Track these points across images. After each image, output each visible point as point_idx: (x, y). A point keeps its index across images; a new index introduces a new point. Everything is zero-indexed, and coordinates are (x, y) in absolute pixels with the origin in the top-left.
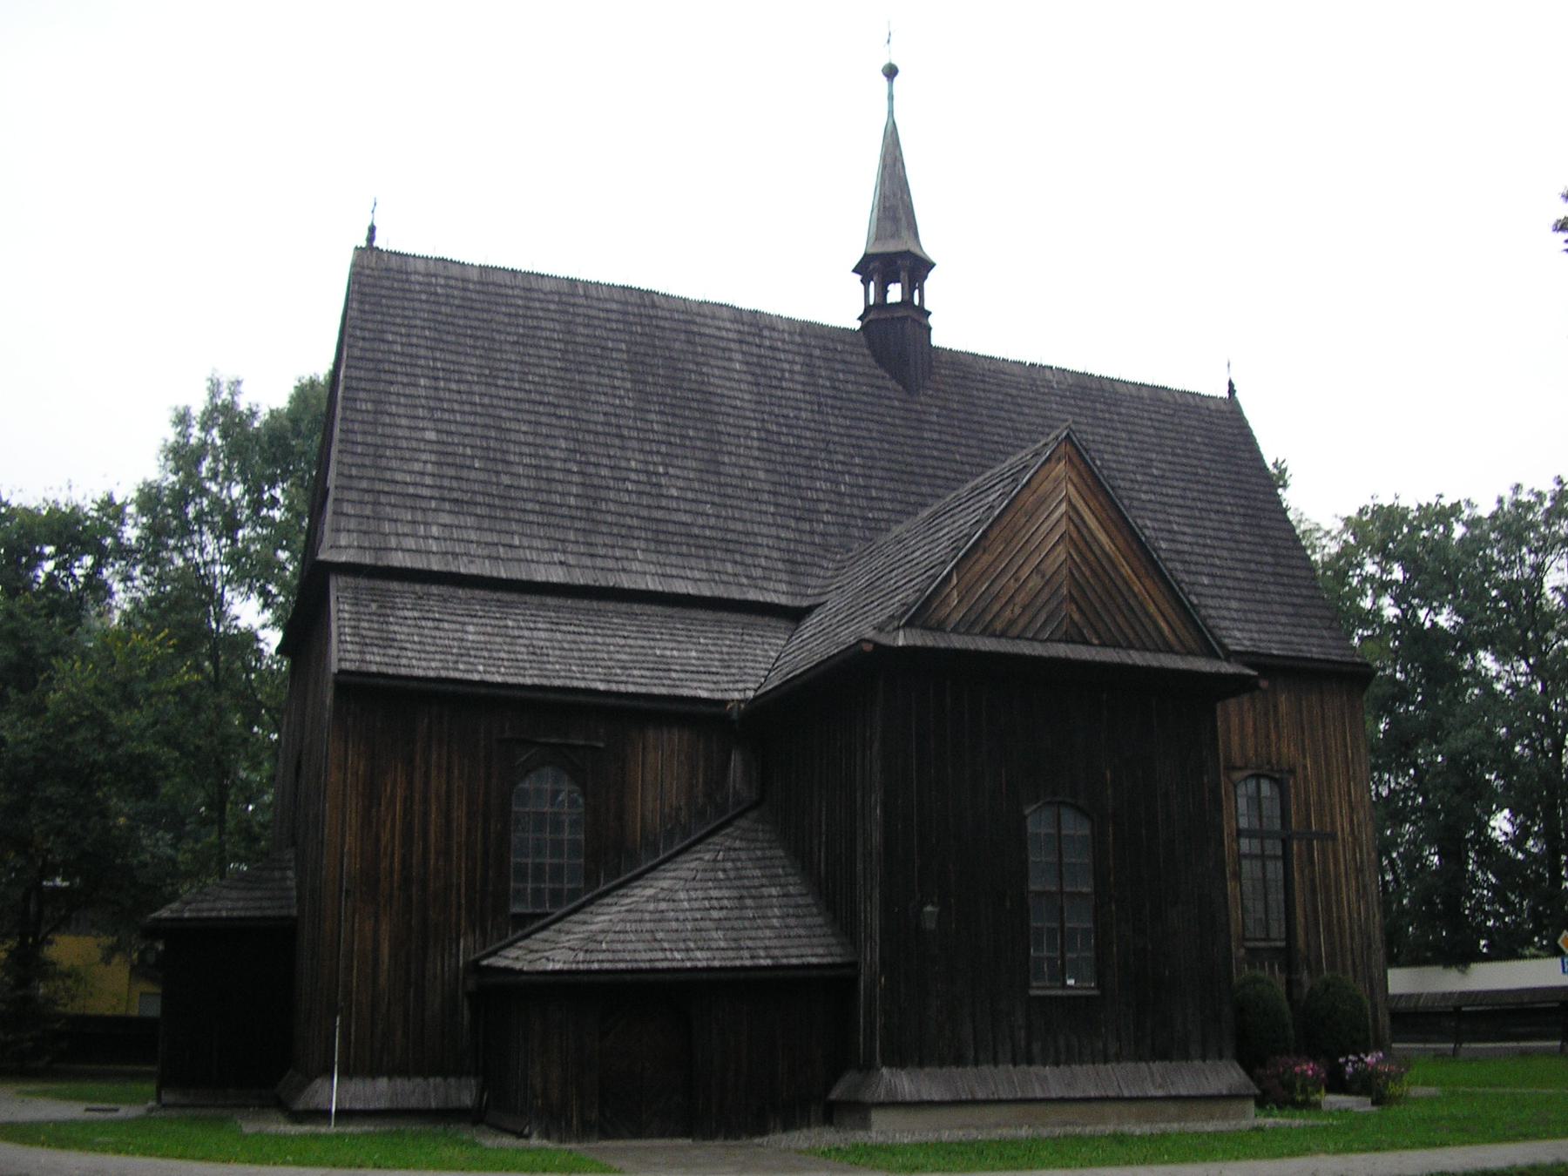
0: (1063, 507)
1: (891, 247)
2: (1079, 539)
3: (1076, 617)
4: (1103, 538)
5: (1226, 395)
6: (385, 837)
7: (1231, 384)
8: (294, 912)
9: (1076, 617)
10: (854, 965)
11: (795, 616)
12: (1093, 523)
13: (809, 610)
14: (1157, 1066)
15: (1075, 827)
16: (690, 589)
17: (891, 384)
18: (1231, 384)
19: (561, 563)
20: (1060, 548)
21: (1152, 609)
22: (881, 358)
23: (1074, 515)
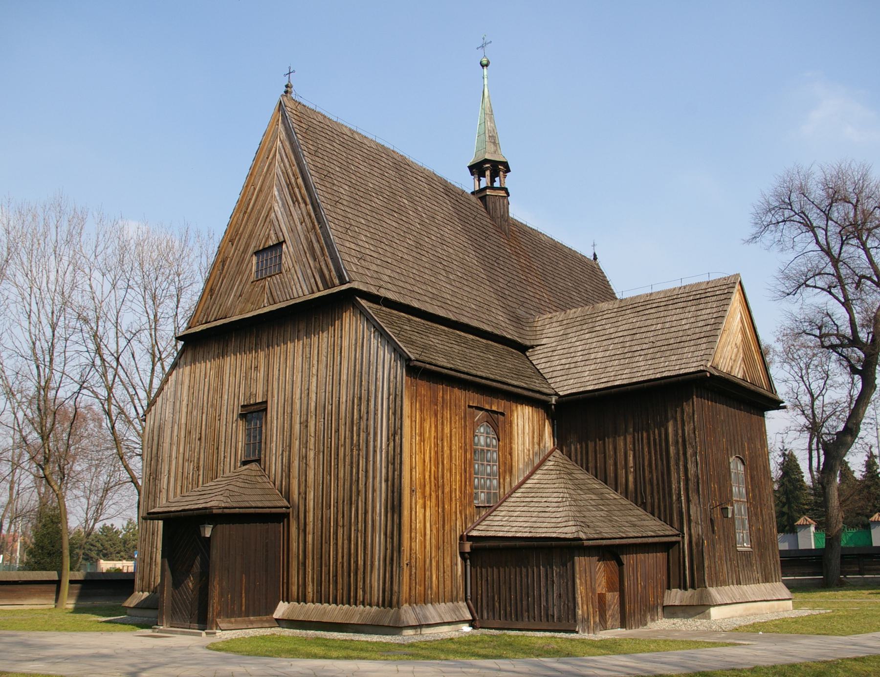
7: (595, 255)
13: (532, 347)
15: (741, 468)
18: (595, 255)
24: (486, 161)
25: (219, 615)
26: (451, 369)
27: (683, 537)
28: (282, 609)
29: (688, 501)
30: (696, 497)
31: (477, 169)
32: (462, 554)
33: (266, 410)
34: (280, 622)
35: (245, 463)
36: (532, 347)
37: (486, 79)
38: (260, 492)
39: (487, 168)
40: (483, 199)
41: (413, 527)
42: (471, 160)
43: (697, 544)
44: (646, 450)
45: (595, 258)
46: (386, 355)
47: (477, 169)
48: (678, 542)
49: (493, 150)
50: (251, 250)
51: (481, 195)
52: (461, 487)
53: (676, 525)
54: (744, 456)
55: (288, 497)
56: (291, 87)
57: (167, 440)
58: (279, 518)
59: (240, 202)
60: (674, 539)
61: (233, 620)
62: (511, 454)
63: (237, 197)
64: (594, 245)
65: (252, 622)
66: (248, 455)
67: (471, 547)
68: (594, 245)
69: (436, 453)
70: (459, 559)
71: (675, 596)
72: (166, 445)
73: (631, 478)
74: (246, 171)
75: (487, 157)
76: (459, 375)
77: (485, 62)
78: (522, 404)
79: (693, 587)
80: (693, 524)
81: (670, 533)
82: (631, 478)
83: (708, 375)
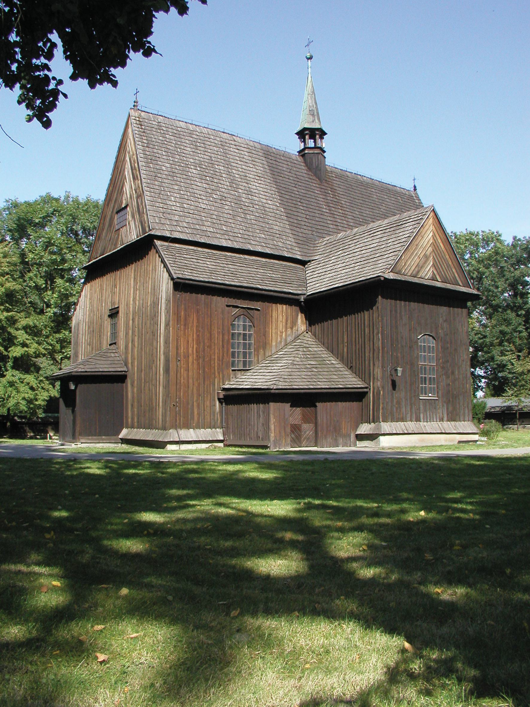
0: (431, 234)
1: (316, 126)
2: (435, 245)
3: (435, 272)
4: (441, 245)
5: (412, 189)
6: (190, 340)
7: (415, 187)
8: (125, 369)
9: (435, 272)
10: (366, 388)
11: (303, 263)
12: (440, 241)
13: (309, 261)
14: (453, 423)
16: (268, 251)
17: (314, 178)
18: (415, 187)
19: (229, 240)
20: (430, 248)
21: (454, 270)
22: (309, 166)
23: (434, 236)
24: (305, 129)
25: (80, 434)
26: (208, 282)
27: (370, 389)
28: (124, 433)
29: (374, 365)
30: (377, 362)
31: (302, 134)
32: (219, 399)
33: (118, 312)
34: (125, 441)
35: (110, 345)
36: (309, 261)
37: (309, 69)
38: (109, 362)
39: (307, 134)
40: (303, 156)
41: (178, 381)
42: (299, 129)
43: (377, 393)
44: (353, 331)
45: (415, 189)
46: (166, 275)
47: (302, 134)
48: (367, 392)
49: (311, 120)
50: (115, 211)
51: (302, 154)
52: (219, 357)
53: (367, 381)
54: (437, 333)
55: (126, 364)
56: (137, 102)
57: (81, 333)
58: (120, 378)
59: (111, 180)
60: (365, 390)
61: (90, 437)
62: (265, 335)
63: (110, 177)
64: (414, 180)
65: (103, 439)
66: (112, 340)
67: (224, 395)
68: (414, 180)
69: (198, 336)
70: (217, 402)
71: (365, 429)
72: (80, 336)
73: (345, 350)
74: (114, 160)
75: (306, 126)
76: (214, 285)
77: (308, 57)
78: (276, 303)
79: (374, 422)
80: (375, 380)
81: (363, 386)
82: (345, 350)
83: (382, 279)
